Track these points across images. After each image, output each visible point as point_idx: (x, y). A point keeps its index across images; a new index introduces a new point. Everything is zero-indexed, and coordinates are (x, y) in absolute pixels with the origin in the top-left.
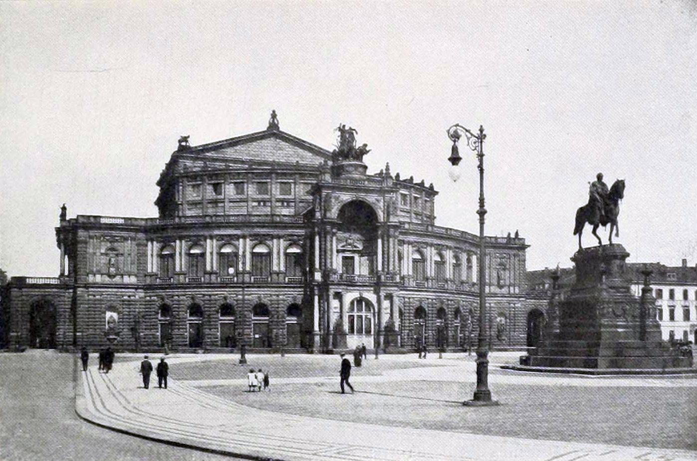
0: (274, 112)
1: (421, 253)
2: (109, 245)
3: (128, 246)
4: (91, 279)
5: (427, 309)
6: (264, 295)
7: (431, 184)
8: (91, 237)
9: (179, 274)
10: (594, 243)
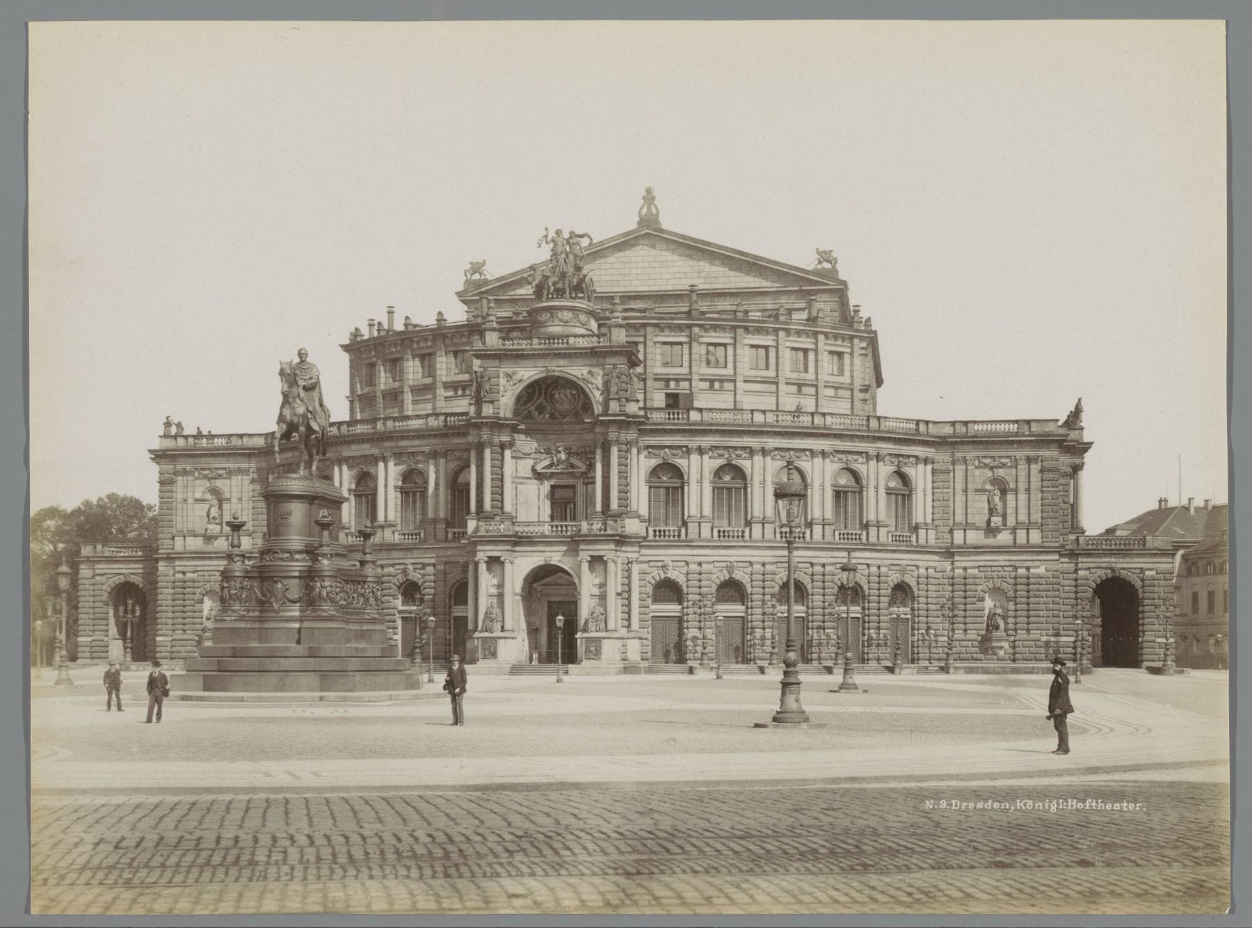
0: (649, 191)
2: (208, 484)
4: (179, 542)
8: (176, 473)
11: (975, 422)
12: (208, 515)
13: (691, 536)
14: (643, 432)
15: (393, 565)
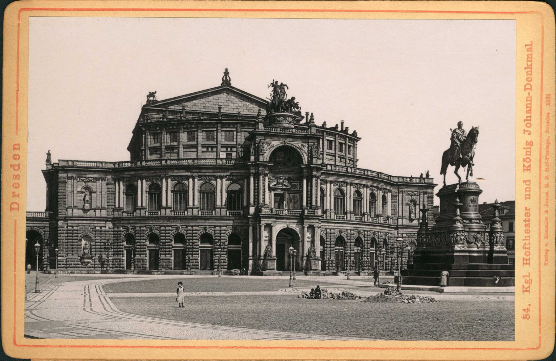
1: (342, 192)
2: (84, 184)
3: (99, 186)
4: (70, 211)
5: (346, 239)
6: (210, 227)
7: (355, 131)
8: (68, 178)
10: (455, 181)
14: (322, 174)
15: (198, 226)
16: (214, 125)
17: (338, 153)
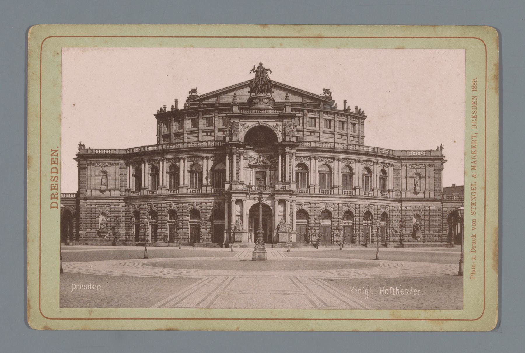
2: (101, 169)
4: (89, 192)
8: (88, 164)
9: (143, 189)
11: (410, 151)
12: (101, 181)
13: (311, 193)
16: (212, 111)
17: (337, 130)
